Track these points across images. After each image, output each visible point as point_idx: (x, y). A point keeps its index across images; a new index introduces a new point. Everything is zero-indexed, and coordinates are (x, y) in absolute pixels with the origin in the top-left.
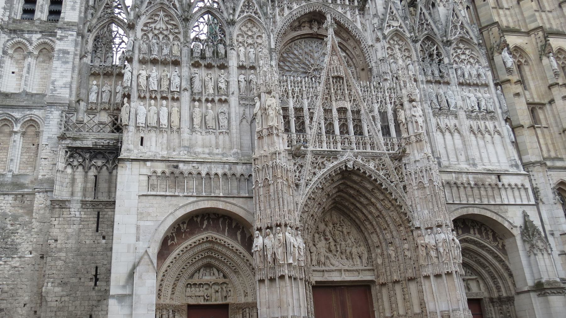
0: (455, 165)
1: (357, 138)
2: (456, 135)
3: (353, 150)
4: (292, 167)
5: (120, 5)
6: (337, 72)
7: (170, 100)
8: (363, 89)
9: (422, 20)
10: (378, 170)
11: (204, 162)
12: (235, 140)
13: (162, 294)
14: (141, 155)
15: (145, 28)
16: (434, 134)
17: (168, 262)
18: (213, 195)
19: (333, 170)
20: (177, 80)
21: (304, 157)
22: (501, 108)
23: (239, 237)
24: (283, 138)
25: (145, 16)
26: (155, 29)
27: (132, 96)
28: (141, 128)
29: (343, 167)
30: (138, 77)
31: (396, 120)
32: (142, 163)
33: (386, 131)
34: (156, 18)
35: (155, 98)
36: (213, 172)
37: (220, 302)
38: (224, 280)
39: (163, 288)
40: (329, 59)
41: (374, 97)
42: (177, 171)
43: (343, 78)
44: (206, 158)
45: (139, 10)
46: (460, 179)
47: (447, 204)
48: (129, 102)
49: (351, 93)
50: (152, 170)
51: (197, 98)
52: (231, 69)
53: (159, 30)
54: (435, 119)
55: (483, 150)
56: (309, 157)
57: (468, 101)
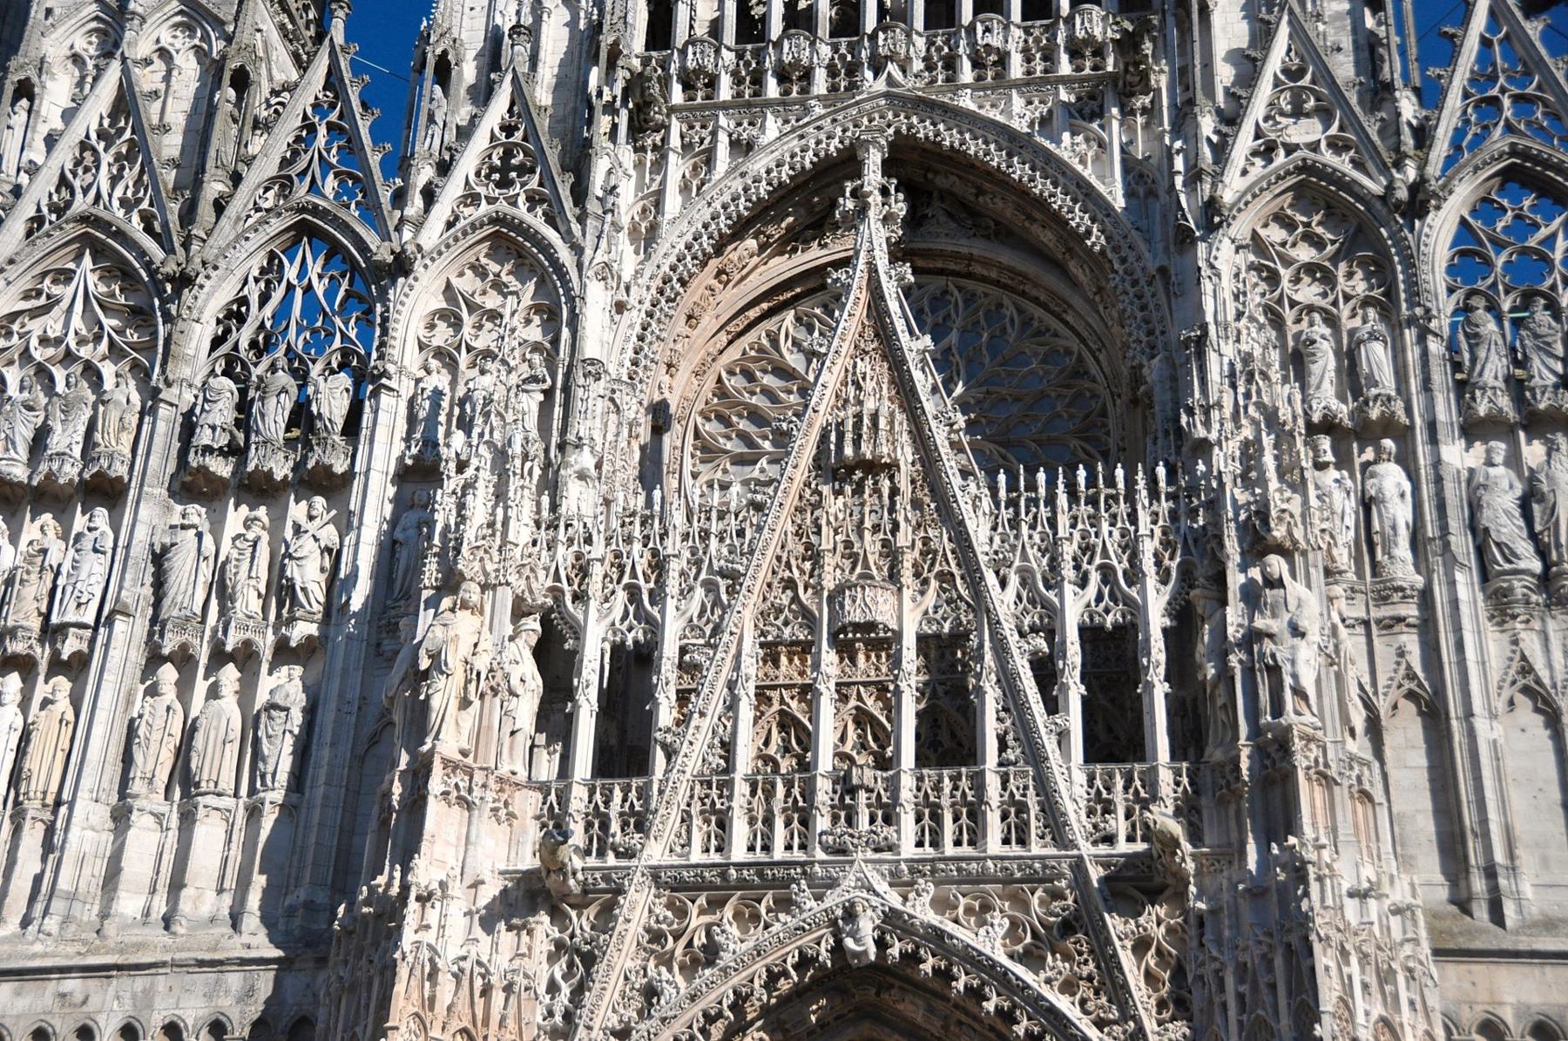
1: (927, 785)
3: (890, 848)
7: (43, 667)
8: (1006, 514)
9: (1493, 79)
10: (1031, 958)
11: (119, 968)
16: (1481, 724)
19: (759, 968)
20: (94, 569)
26: (44, 341)
34: (57, 290)
36: (157, 1020)
40: (831, 378)
41: (1069, 550)
43: (892, 468)
44: (140, 946)
51: (169, 645)
54: (1506, 637)
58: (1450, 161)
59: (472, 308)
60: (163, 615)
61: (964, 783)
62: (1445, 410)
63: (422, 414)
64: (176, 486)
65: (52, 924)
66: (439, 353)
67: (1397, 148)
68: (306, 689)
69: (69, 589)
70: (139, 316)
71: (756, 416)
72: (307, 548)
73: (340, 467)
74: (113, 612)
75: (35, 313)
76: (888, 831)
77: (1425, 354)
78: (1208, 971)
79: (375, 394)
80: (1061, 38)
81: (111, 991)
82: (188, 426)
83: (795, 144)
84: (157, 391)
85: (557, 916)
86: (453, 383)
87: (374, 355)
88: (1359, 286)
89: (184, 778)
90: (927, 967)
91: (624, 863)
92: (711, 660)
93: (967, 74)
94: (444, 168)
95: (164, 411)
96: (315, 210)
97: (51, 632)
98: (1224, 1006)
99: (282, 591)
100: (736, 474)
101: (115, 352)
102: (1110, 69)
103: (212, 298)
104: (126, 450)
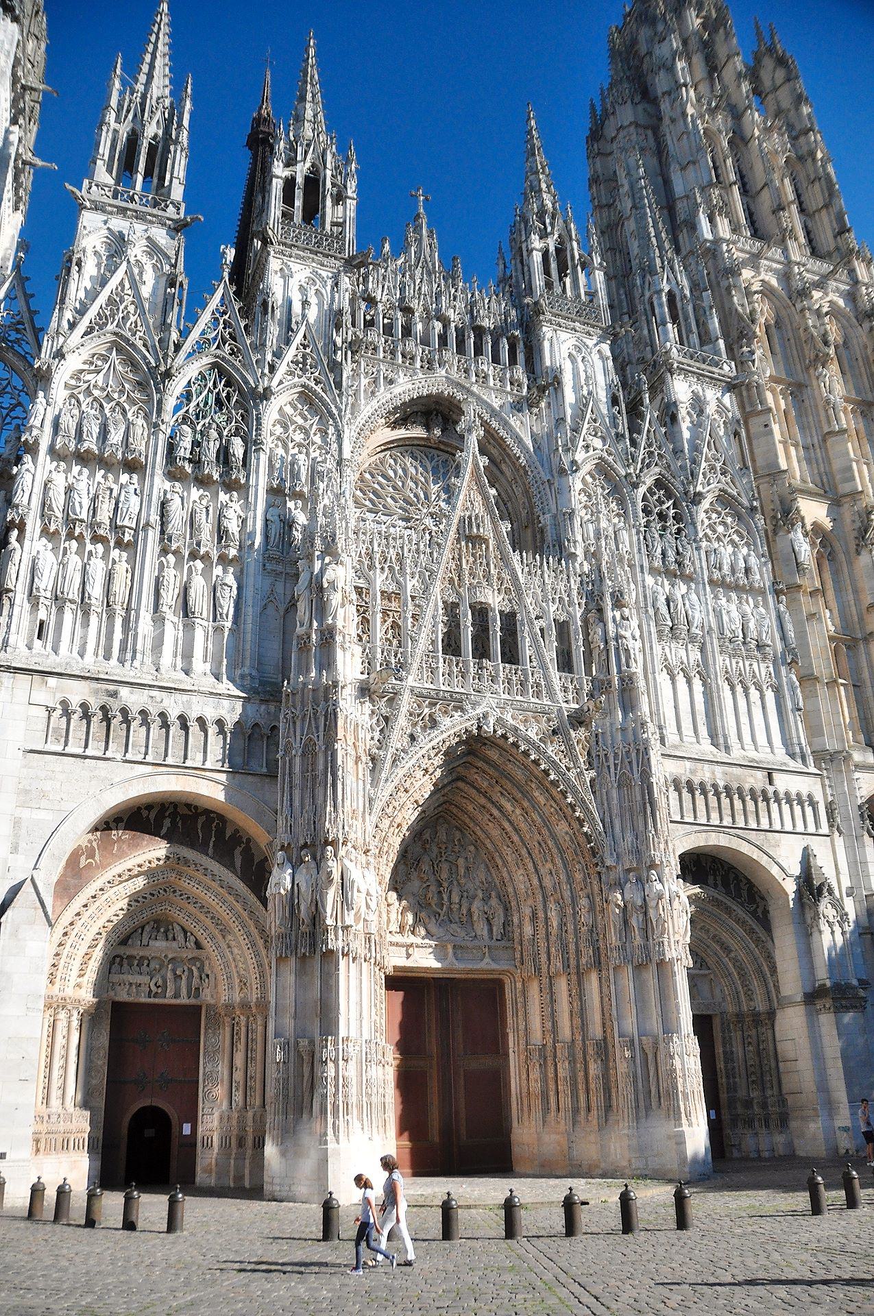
0: (691, 743)
2: (697, 684)
4: (367, 717)
5: (23, 324)
6: (478, 527)
8: (526, 569)
11: (175, 689)
12: (248, 646)
13: (59, 975)
14: (37, 660)
15: (73, 382)
16: (657, 675)
17: (76, 904)
18: (189, 763)
20: (134, 501)
21: (391, 700)
22: (784, 638)
23: (238, 861)
24: (353, 655)
25: (76, 354)
27: (29, 528)
28: (42, 599)
29: (474, 727)
30: (46, 485)
31: (587, 643)
32: (36, 677)
33: (565, 663)
34: (99, 363)
35: (80, 538)
37: (184, 1000)
38: (196, 953)
39: (62, 962)
42: (115, 706)
43: (486, 541)
44: (181, 681)
45: (65, 341)
46: (699, 774)
47: (671, 822)
48: (20, 539)
49: (503, 575)
50: (59, 697)
52: (252, 491)
53: (103, 389)
55: (744, 719)
56: (406, 702)
57: (725, 618)
58: (641, 471)
59: (293, 422)
60: (169, 530)
61: (520, 673)
62: (646, 564)
63: (278, 466)
64: (166, 472)
65: (137, 663)
66: (278, 439)
67: (628, 460)
68: (236, 578)
69: (125, 510)
70: (141, 385)
71: (375, 493)
72: (230, 514)
73: (243, 481)
74: (147, 524)
75: (90, 372)
76: (496, 686)
77: (639, 539)
78: (602, 754)
79: (257, 451)
80: (508, 376)
81: (172, 698)
82: (171, 448)
83: (410, 386)
84: (156, 425)
85: (372, 701)
86: (287, 452)
87: (254, 433)
88: (613, 506)
89: (186, 610)
90: (511, 740)
91: (398, 682)
92: (428, 605)
93: (474, 379)
94: (278, 355)
95: (161, 436)
96: (223, 359)
97: (116, 528)
98: (608, 767)
99: (221, 534)
100: (370, 516)
101: (132, 402)
102: (524, 394)
103: (177, 387)
104: (143, 448)
